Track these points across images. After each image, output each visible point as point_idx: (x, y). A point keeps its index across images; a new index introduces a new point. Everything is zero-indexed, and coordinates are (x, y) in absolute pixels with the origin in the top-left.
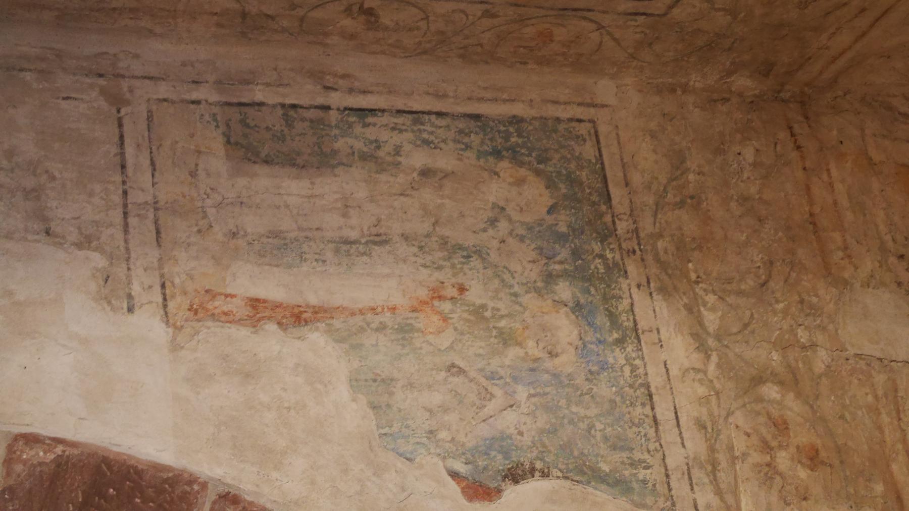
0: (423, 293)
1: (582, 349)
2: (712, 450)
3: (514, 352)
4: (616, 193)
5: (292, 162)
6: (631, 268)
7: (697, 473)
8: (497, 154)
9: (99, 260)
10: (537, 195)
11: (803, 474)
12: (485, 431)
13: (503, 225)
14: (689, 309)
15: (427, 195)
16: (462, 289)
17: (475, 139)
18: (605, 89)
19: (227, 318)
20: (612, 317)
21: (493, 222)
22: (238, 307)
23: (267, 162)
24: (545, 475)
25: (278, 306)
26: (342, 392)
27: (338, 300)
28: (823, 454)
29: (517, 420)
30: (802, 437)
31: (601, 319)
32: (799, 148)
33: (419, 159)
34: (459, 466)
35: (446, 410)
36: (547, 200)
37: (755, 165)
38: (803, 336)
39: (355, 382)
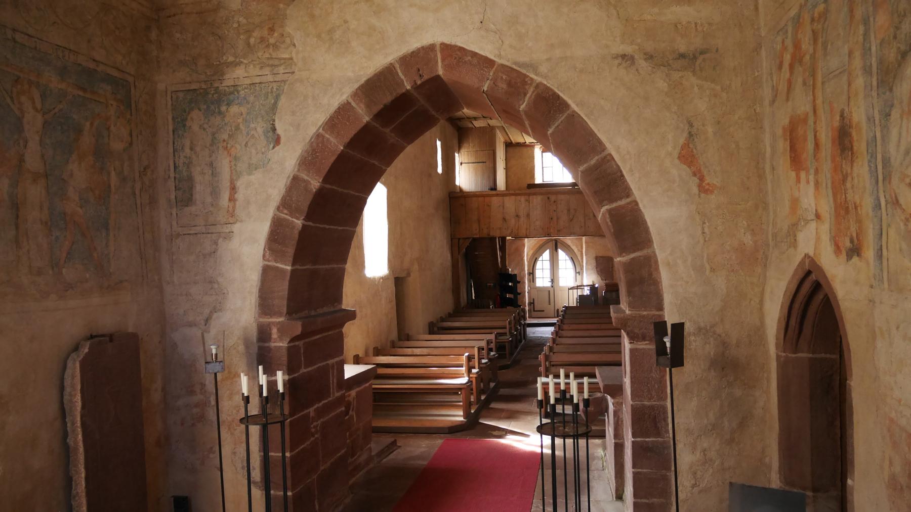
0: (226, 153)
1: (240, 104)
2: (268, 65)
3: (241, 126)
4: (193, 87)
5: (191, 188)
6: (216, 85)
7: (275, 72)
8: (184, 126)
9: (221, 240)
10: (195, 114)
11: (276, 34)
12: (262, 138)
13: (205, 126)
14: (227, 67)
15: (198, 149)
16: (224, 141)
17: (180, 132)
18: (161, 87)
19: (234, 207)
20: (232, 93)
21: (204, 129)
22: (231, 204)
23: (192, 195)
24: (274, 121)
25: (230, 194)
26: (252, 177)
27: (228, 177)
28: (271, 26)
29: (259, 127)
30: (265, 32)
31: (231, 97)
32: (174, 15)
33: (187, 150)
34: (271, 146)
35: (256, 149)
36: (196, 111)
37: (181, 33)
38: (235, 25)
39: (250, 174)
